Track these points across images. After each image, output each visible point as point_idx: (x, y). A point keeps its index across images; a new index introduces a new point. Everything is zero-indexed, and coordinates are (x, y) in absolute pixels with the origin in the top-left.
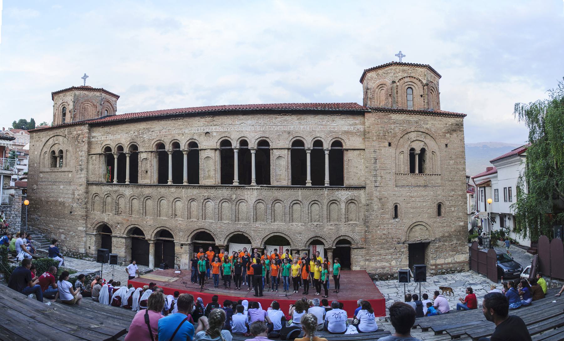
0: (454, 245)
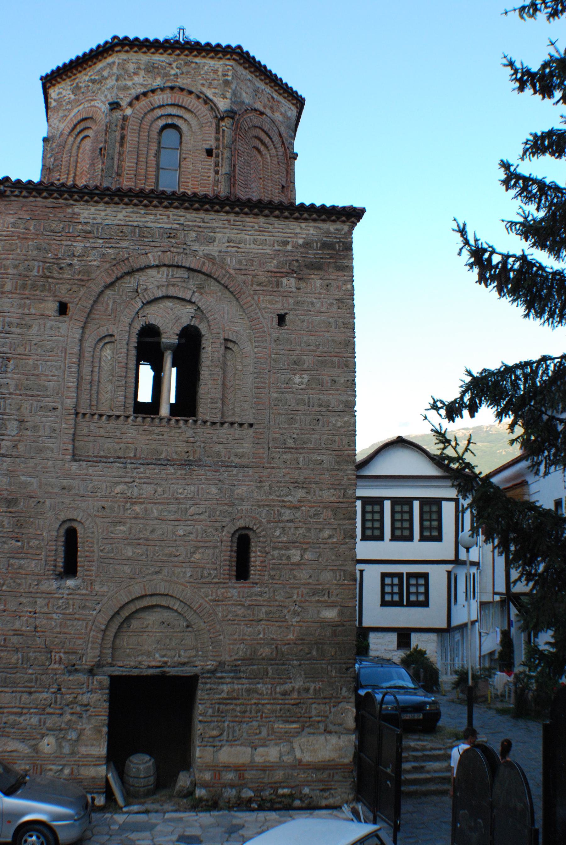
0: (295, 695)
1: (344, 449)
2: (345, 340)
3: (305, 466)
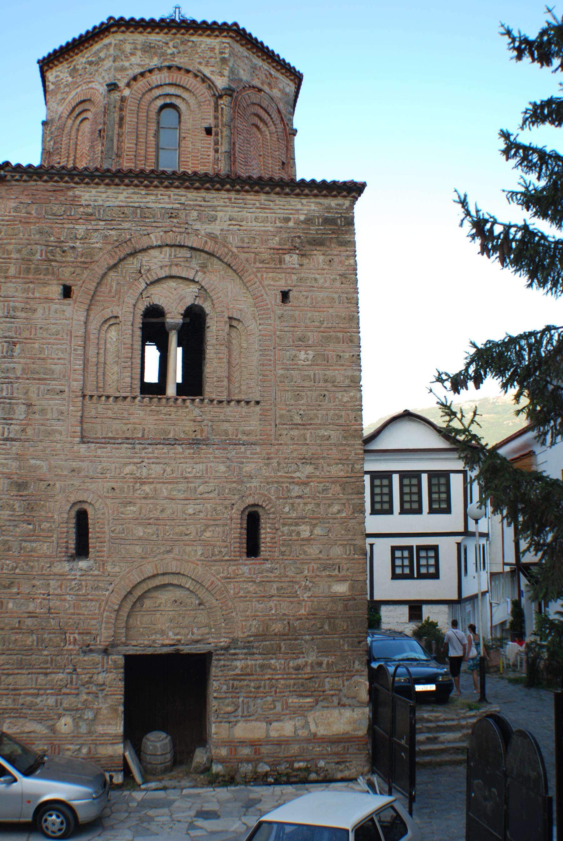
0: (308, 670)
1: (351, 424)
2: (349, 316)
3: (313, 442)
